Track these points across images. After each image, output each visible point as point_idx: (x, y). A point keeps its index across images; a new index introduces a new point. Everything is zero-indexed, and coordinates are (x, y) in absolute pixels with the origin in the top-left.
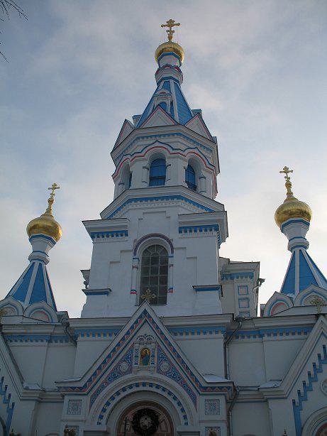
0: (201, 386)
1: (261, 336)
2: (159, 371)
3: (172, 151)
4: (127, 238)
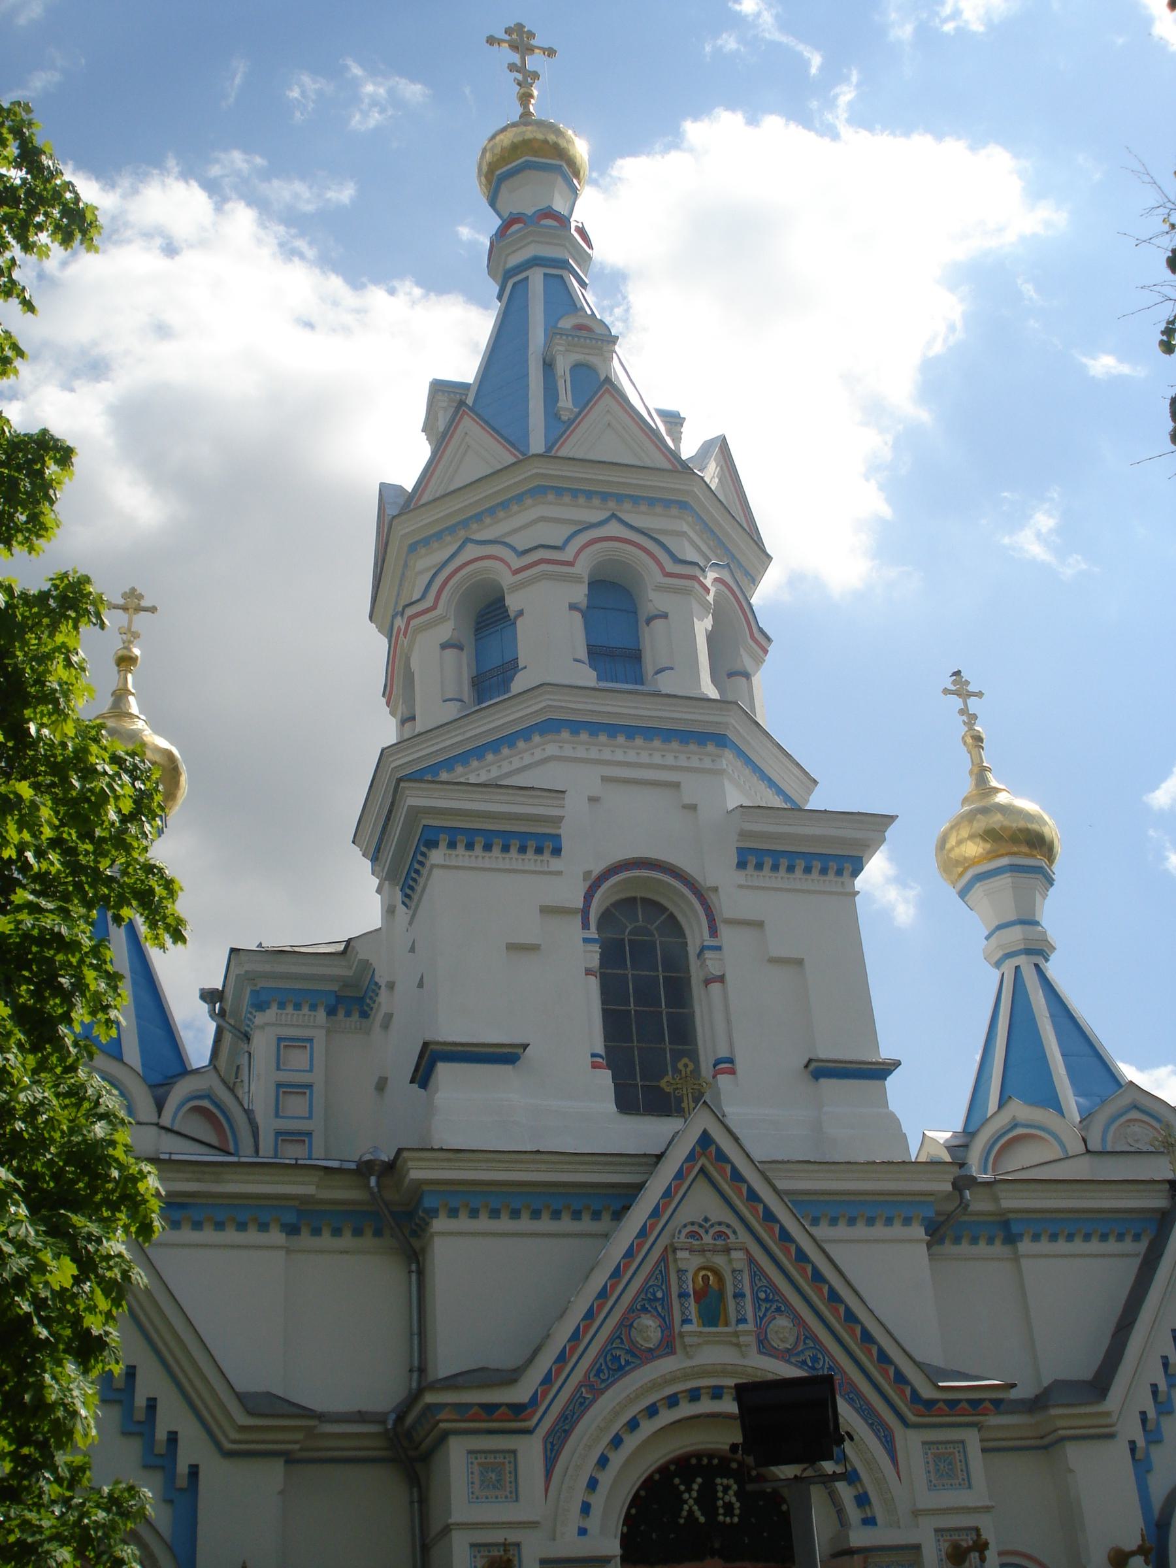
0: (916, 1397)
1: (1011, 1239)
2: (764, 1345)
3: (670, 567)
4: (555, 864)
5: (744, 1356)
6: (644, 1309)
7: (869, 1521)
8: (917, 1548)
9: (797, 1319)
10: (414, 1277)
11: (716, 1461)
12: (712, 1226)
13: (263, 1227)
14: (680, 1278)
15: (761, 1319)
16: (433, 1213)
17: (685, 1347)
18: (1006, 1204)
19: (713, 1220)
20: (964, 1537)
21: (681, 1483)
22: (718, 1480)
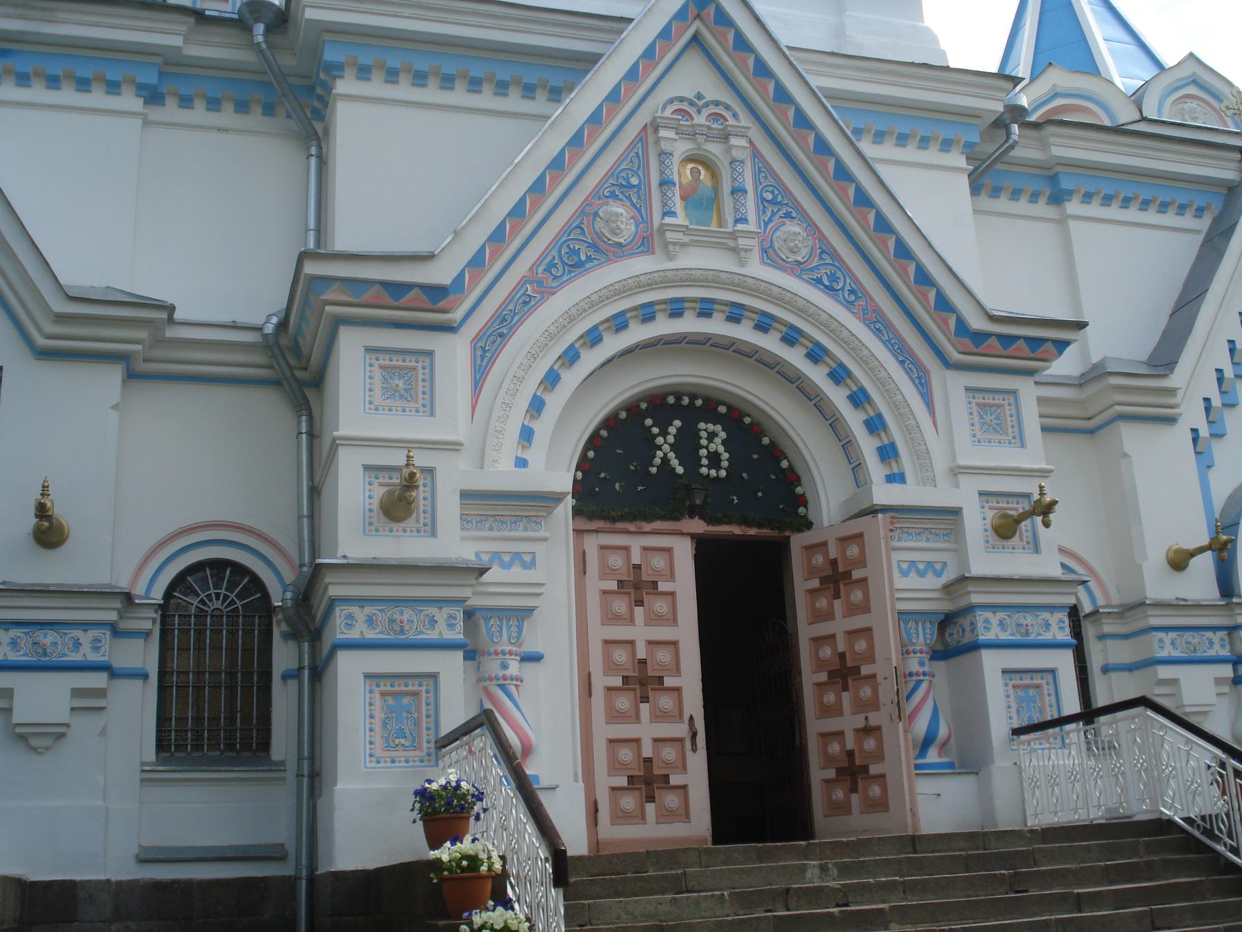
0: (962, 326)
1: (1057, 198)
2: (769, 255)
5: (742, 263)
6: (613, 196)
7: (896, 478)
8: (956, 512)
9: (811, 226)
10: (313, 161)
11: (699, 402)
12: (707, 105)
13: (113, 87)
14: (662, 163)
15: (766, 224)
16: (336, 70)
17: (666, 244)
18: (1057, 151)
19: (710, 95)
20: (1015, 506)
21: (653, 425)
22: (702, 425)
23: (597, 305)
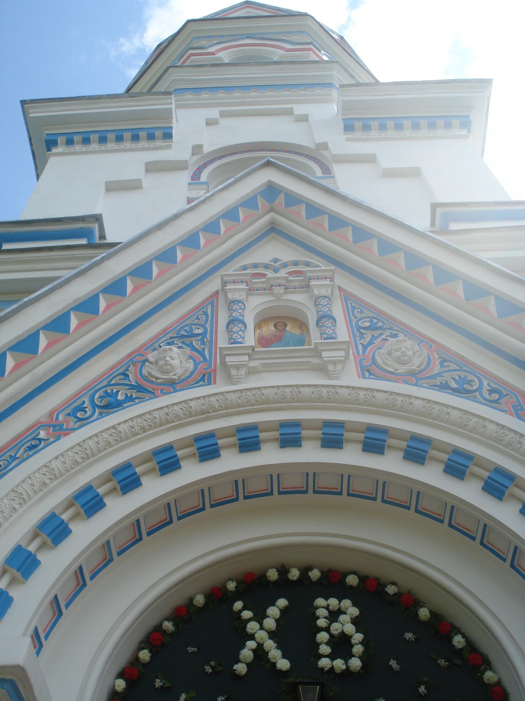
11: (315, 574)
15: (365, 347)
21: (244, 608)
22: (320, 602)
23: (127, 438)
